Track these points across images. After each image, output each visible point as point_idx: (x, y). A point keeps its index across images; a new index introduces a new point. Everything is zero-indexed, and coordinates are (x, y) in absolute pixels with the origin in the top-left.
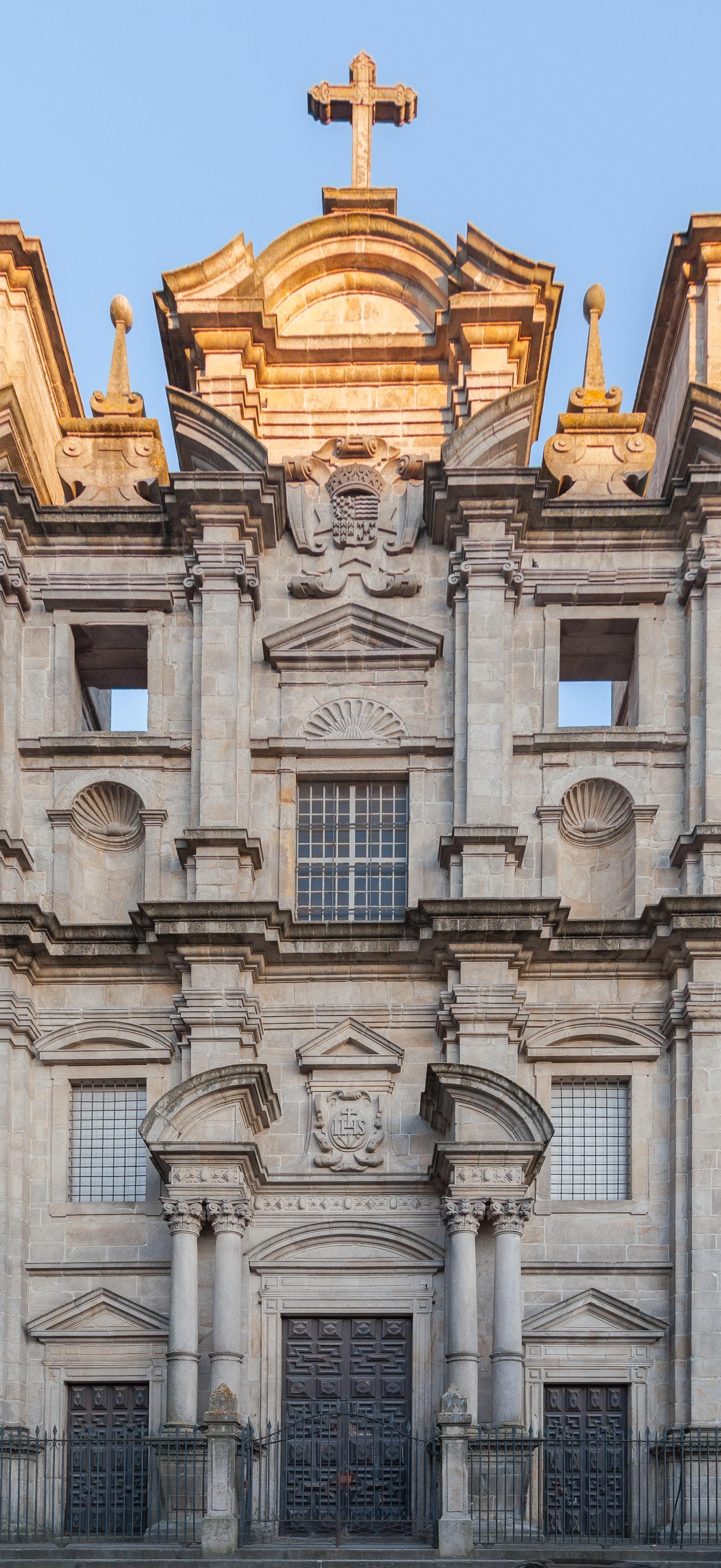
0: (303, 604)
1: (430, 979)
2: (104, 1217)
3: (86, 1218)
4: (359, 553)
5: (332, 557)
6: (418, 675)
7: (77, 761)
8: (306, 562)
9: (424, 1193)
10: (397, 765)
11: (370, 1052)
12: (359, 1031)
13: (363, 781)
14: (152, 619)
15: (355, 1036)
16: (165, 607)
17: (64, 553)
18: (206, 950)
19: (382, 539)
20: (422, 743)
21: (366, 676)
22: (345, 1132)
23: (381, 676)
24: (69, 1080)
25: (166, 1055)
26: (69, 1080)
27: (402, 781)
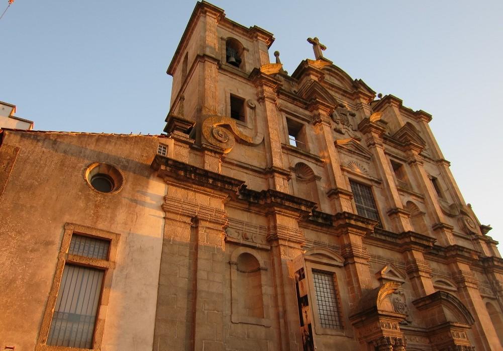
0: (337, 134)
1: (399, 252)
2: (334, 337)
3: (328, 337)
4: (347, 127)
5: (340, 124)
6: (367, 161)
7: (294, 154)
8: (336, 124)
9: (424, 336)
10: (369, 183)
11: (396, 276)
12: (393, 268)
13: (361, 184)
14: (306, 123)
15: (392, 270)
16: (308, 122)
17: (281, 99)
18: (355, 230)
19: (350, 126)
20: (376, 180)
21: (356, 157)
22: (400, 307)
23: (360, 158)
24: (312, 269)
25: (342, 265)
26: (312, 269)
27: (369, 188)
